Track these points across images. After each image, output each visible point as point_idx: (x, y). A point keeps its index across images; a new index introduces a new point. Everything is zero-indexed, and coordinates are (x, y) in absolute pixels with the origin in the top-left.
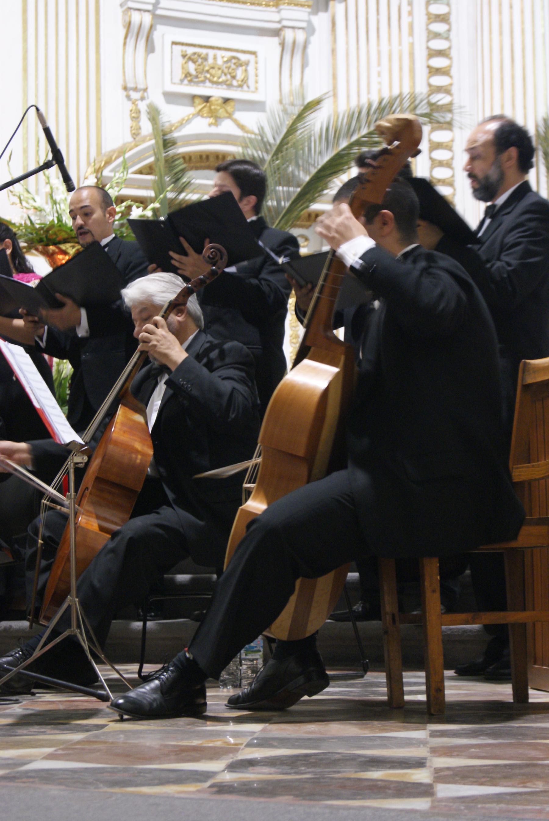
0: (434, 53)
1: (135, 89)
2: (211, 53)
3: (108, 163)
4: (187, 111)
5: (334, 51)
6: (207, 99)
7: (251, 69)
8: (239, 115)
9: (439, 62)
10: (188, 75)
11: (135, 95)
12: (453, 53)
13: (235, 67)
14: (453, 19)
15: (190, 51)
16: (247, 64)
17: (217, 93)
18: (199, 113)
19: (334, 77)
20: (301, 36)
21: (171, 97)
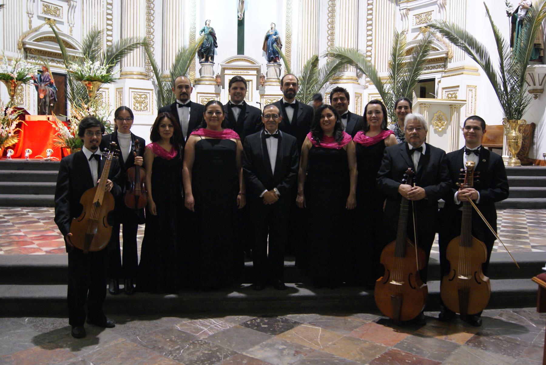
0: (108, 14)
1: (31, 14)
2: (51, 5)
3: (25, 37)
4: (43, 22)
5: (83, 10)
6: (49, 19)
7: (61, 11)
8: (57, 25)
9: (109, 17)
10: (45, 11)
11: (30, 16)
12: (113, 15)
13: (57, 11)
14: (113, 5)
15: (45, 4)
16: (60, 10)
17: (52, 18)
18: (47, 23)
19: (83, 17)
20: (75, 4)
21: (39, 17)
